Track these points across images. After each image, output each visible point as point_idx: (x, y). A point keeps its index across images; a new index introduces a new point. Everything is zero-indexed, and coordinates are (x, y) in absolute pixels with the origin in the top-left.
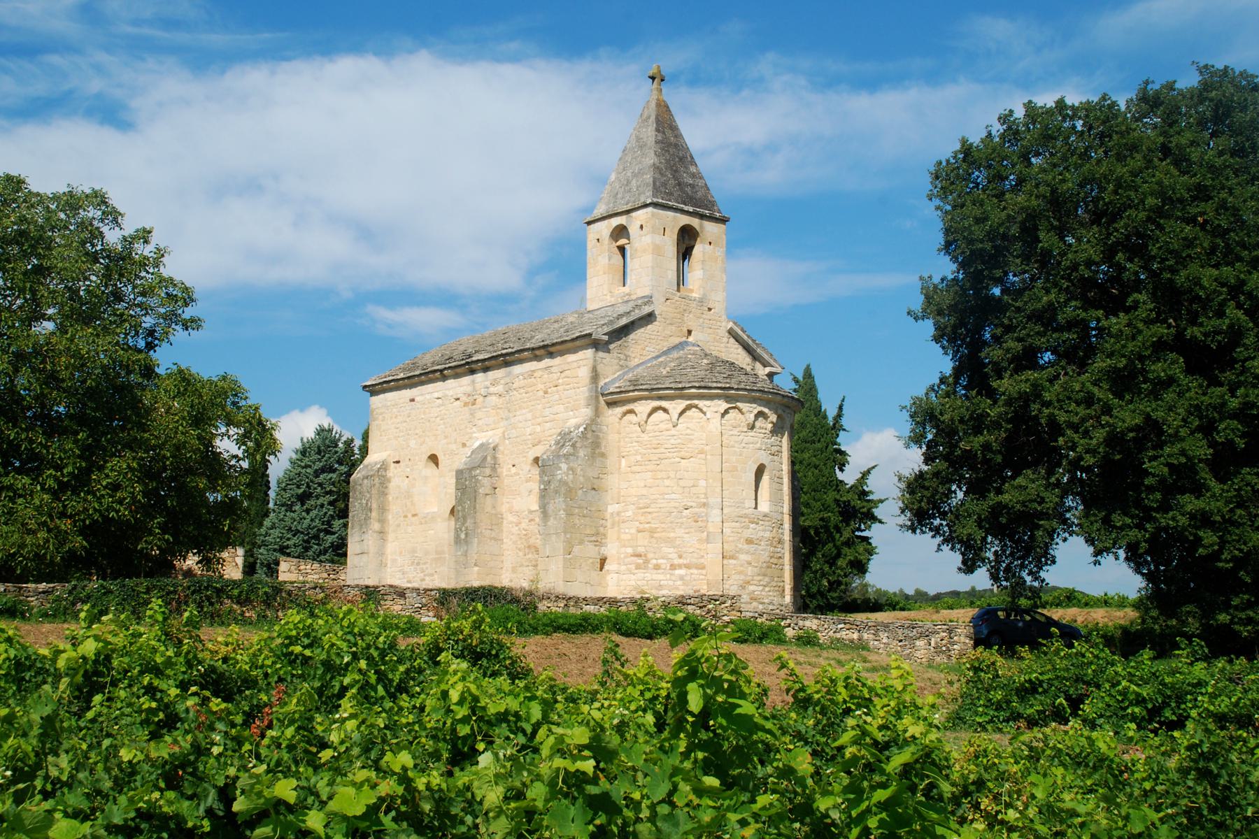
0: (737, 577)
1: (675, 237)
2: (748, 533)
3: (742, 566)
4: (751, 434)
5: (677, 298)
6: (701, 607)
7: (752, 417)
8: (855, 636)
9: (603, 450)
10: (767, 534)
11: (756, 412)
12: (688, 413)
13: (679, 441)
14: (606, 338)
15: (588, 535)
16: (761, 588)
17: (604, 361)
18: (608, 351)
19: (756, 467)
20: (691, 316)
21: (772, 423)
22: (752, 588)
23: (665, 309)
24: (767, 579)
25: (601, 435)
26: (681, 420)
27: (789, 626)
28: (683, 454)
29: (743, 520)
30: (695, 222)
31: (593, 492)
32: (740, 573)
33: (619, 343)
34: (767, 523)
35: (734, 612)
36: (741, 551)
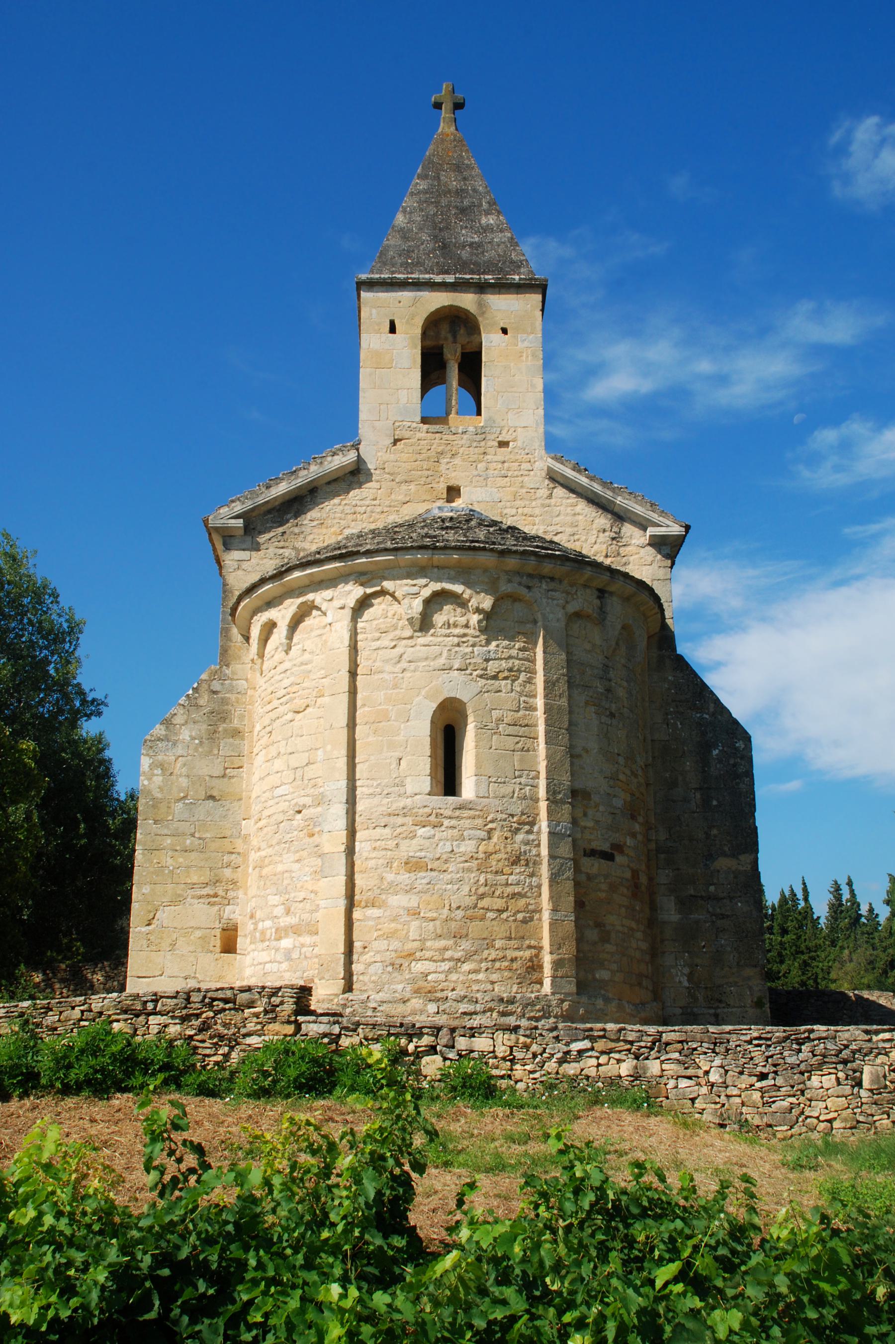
0: (382, 945)
1: (419, 331)
2: (409, 849)
3: (394, 919)
4: (427, 639)
5: (423, 435)
6: (184, 1019)
7: (417, 605)
8: (625, 1069)
9: (236, 723)
10: (468, 847)
11: (426, 593)
12: (308, 622)
13: (292, 679)
14: (240, 522)
15: (193, 886)
16: (446, 966)
17: (245, 565)
18: (256, 548)
19: (434, 705)
20: (457, 461)
21: (478, 610)
22: (419, 967)
23: (392, 457)
24: (465, 945)
25: (233, 697)
26: (296, 639)
27: (432, 1050)
28: (299, 703)
29: (400, 820)
30: (467, 301)
31: (211, 803)
32: (388, 936)
33: (281, 530)
34: (467, 823)
35: (275, 1027)
36: (393, 888)
